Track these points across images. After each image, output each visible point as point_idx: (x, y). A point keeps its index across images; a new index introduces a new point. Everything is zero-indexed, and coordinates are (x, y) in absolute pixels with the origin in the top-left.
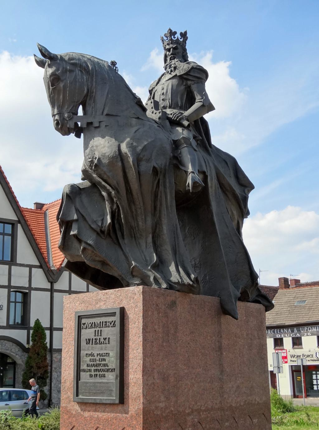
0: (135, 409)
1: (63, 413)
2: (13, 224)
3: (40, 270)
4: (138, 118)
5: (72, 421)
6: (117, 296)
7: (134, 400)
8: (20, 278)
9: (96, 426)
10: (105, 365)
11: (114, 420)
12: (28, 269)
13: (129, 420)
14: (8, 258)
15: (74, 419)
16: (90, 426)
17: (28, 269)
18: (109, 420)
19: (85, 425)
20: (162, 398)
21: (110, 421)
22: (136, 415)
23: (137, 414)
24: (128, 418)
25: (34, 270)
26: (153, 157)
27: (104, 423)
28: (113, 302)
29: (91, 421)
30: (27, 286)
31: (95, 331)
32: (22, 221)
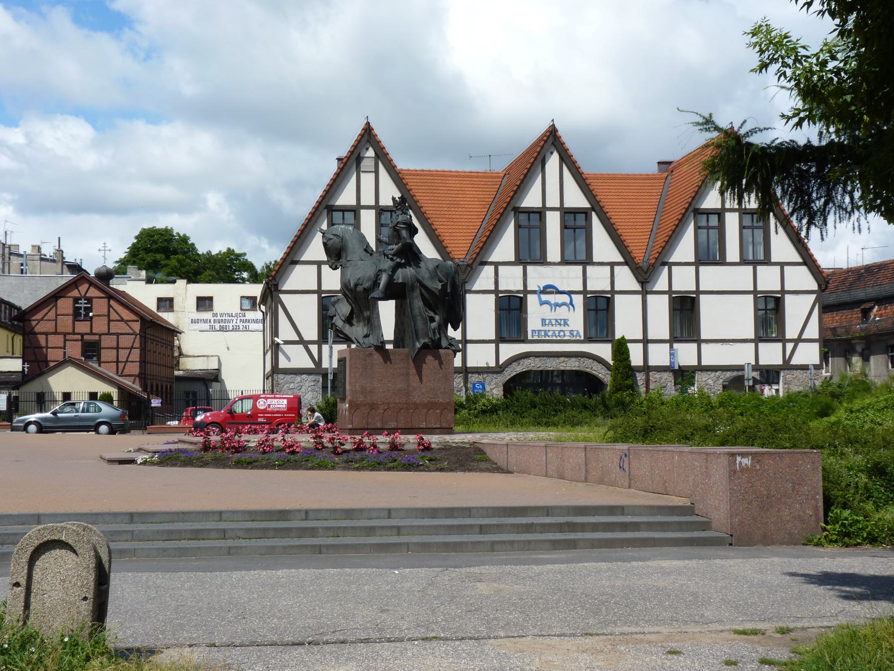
2: (585, 212)
3: (626, 268)
8: (598, 280)
12: (608, 268)
14: (582, 256)
17: (608, 268)
25: (616, 268)
30: (609, 289)
32: (597, 208)
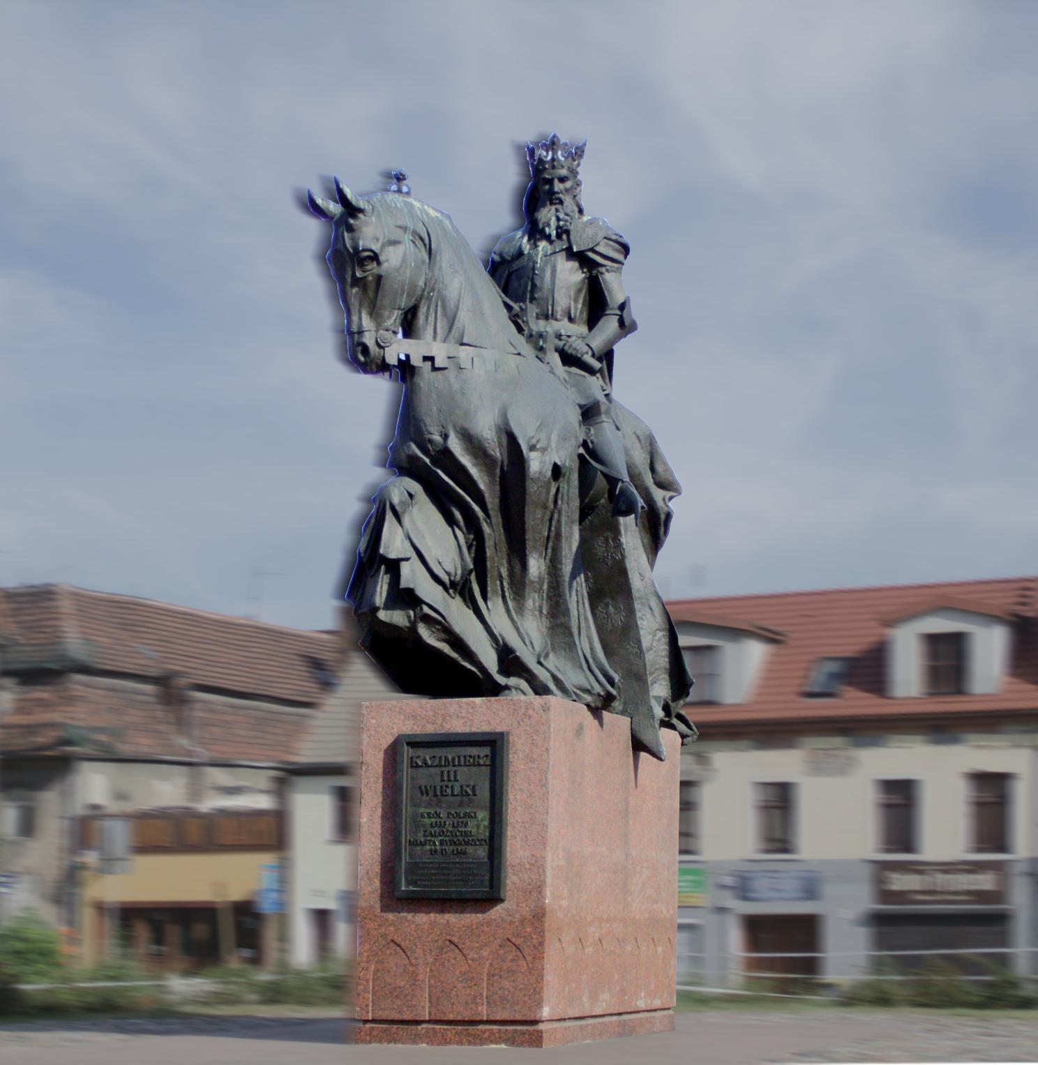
0: (530, 908)
1: (365, 918)
4: (519, 354)
5: (387, 932)
6: (495, 710)
7: (528, 893)
9: (444, 938)
10: (466, 834)
11: (485, 927)
13: (517, 926)
15: (392, 928)
16: (429, 939)
18: (474, 927)
19: (419, 938)
20: (566, 894)
21: (477, 928)
22: (531, 917)
23: (534, 917)
24: (514, 924)
26: (553, 445)
27: (461, 933)
28: (485, 721)
29: (431, 931)
31: (442, 772)
